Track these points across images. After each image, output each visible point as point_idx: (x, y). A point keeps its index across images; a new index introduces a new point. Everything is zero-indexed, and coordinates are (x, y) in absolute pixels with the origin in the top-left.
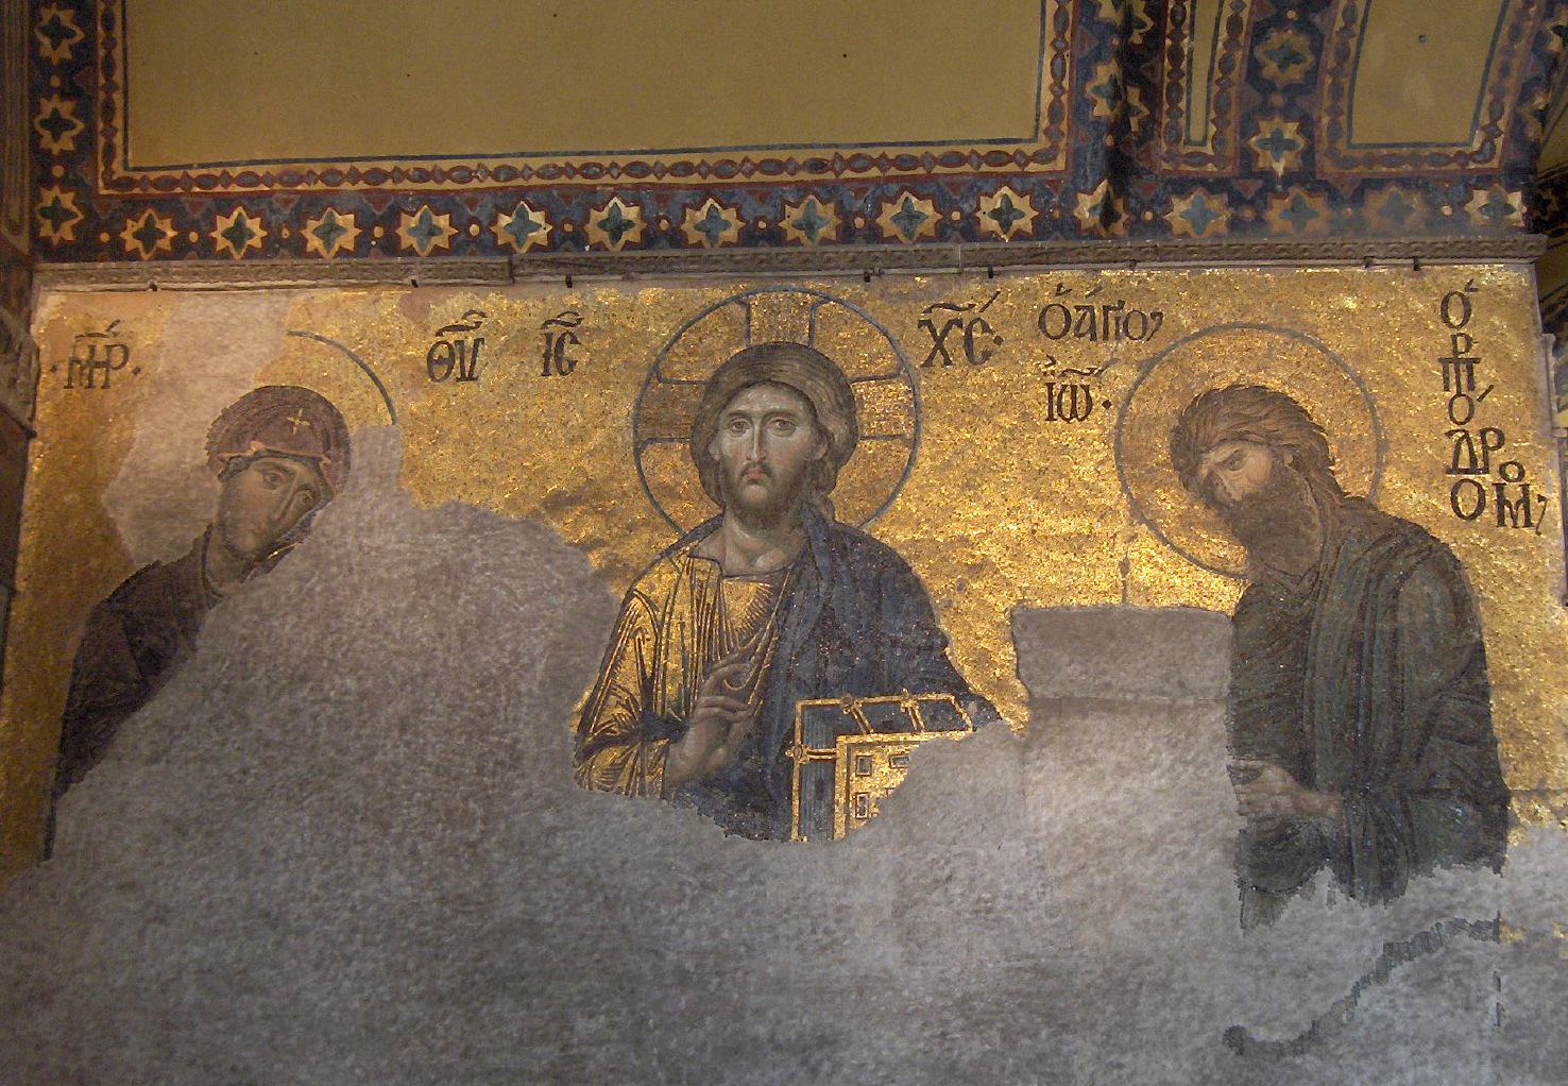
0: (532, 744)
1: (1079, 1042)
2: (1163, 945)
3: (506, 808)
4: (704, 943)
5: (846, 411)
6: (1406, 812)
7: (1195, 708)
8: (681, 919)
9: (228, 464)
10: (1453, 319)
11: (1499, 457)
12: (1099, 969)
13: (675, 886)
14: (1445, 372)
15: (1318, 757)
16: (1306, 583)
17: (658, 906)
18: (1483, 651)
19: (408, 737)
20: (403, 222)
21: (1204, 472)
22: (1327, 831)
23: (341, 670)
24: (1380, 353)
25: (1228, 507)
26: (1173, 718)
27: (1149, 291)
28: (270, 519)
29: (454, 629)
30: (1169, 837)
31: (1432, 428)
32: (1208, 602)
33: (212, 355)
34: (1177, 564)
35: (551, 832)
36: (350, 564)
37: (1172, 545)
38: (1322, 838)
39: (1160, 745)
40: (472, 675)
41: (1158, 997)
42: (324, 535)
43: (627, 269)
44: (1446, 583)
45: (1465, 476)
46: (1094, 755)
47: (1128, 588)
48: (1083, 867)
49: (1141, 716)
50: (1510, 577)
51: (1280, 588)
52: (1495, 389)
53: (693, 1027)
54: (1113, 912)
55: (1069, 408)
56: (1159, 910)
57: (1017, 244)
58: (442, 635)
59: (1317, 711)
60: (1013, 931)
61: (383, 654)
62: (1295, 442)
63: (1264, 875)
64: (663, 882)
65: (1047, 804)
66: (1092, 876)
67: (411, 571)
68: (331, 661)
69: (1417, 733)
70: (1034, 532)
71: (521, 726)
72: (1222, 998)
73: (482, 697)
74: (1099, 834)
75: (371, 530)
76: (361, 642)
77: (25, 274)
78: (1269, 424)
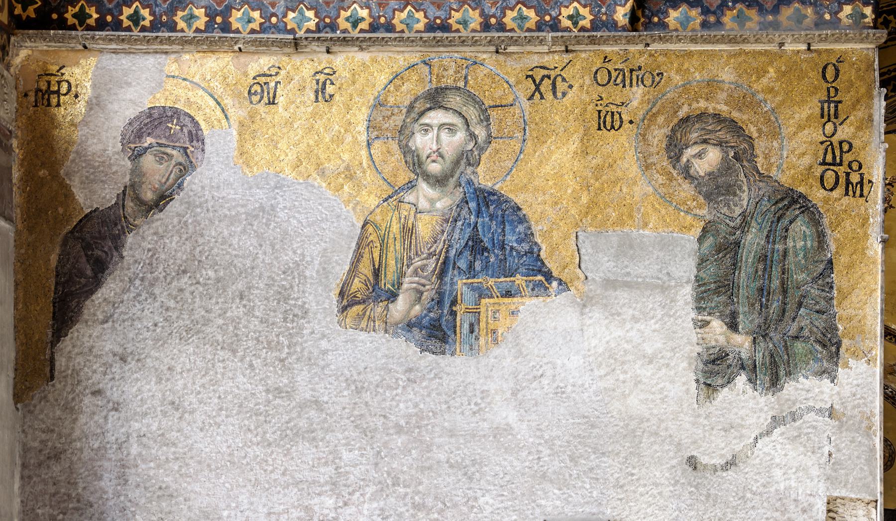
0: (314, 304)
1: (610, 461)
2: (655, 412)
3: (299, 339)
4: (410, 411)
5: (485, 123)
7: (675, 286)
8: (397, 398)
9: (134, 151)
12: (622, 424)
13: (394, 380)
16: (738, 221)
17: (385, 392)
19: (244, 302)
20: (233, 14)
23: (205, 266)
25: (697, 179)
26: (663, 292)
28: (160, 182)
29: (268, 242)
33: (122, 87)
35: (325, 352)
36: (207, 207)
40: (279, 268)
41: (652, 439)
42: (192, 191)
43: (361, 44)
46: (620, 311)
48: (613, 371)
53: (405, 456)
54: (629, 395)
56: (654, 393)
57: (582, 34)
58: (261, 246)
60: (576, 404)
61: (228, 256)
64: (387, 379)
65: (595, 335)
66: (618, 375)
67: (242, 210)
68: (200, 261)
71: (307, 295)
72: (686, 441)
73: (285, 279)
74: (622, 353)
75: (218, 187)
76: (216, 250)
77: (5, 36)
78: (722, 135)
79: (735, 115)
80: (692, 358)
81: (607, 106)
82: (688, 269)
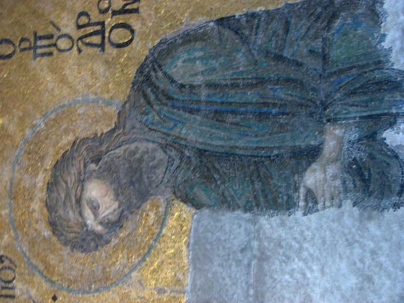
6: (341, 71)
14: (43, 55)
15: (297, 144)
18: (222, 19)
21: (99, 228)
22: (354, 135)
25: (122, 212)
26: (267, 258)
30: (359, 264)
32: (185, 228)
38: (360, 140)
39: (287, 270)
49: (265, 284)
59: (263, 145)
62: (82, 162)
63: (390, 187)
69: (282, 66)
78: (71, 179)
79: (49, 163)
80: (361, 215)
82: (236, 222)
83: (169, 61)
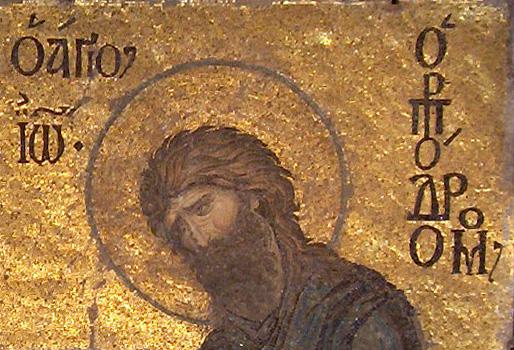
10: (427, 58)
11: (460, 203)
14: (415, 114)
16: (265, 329)
21: (172, 217)
24: (351, 93)
25: (194, 253)
27: (122, 23)
31: (397, 174)
34: (143, 310)
37: (138, 291)
44: (398, 329)
45: (426, 223)
47: (96, 334)
50: (459, 323)
51: (240, 334)
52: (462, 132)
55: (41, 149)
62: (262, 187)
70: (6, 277)
78: (237, 168)
81: (36, 113)
83: (384, 320)
